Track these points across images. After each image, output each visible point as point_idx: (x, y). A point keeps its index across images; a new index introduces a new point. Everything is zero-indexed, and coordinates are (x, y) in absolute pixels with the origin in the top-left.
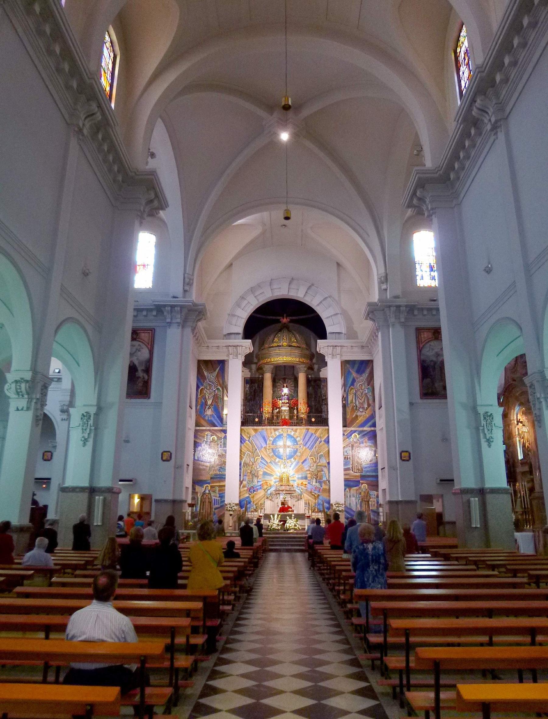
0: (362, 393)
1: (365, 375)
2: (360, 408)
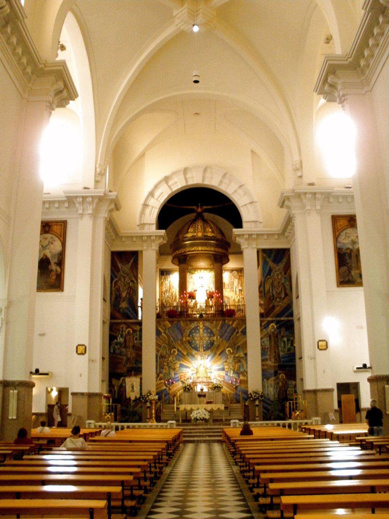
0: (279, 283)
1: (281, 265)
2: (276, 298)
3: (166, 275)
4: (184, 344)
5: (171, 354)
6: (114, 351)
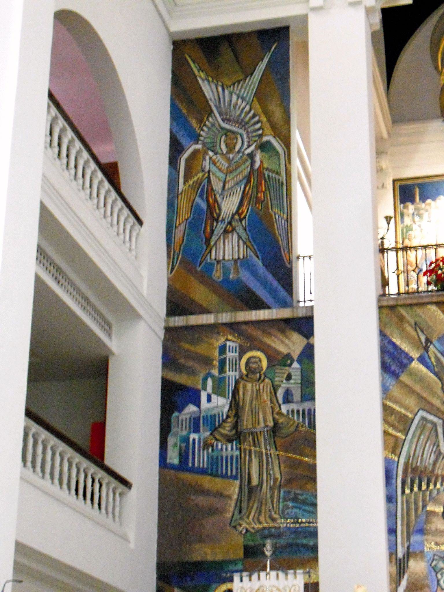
3: (423, 199)
6: (184, 456)
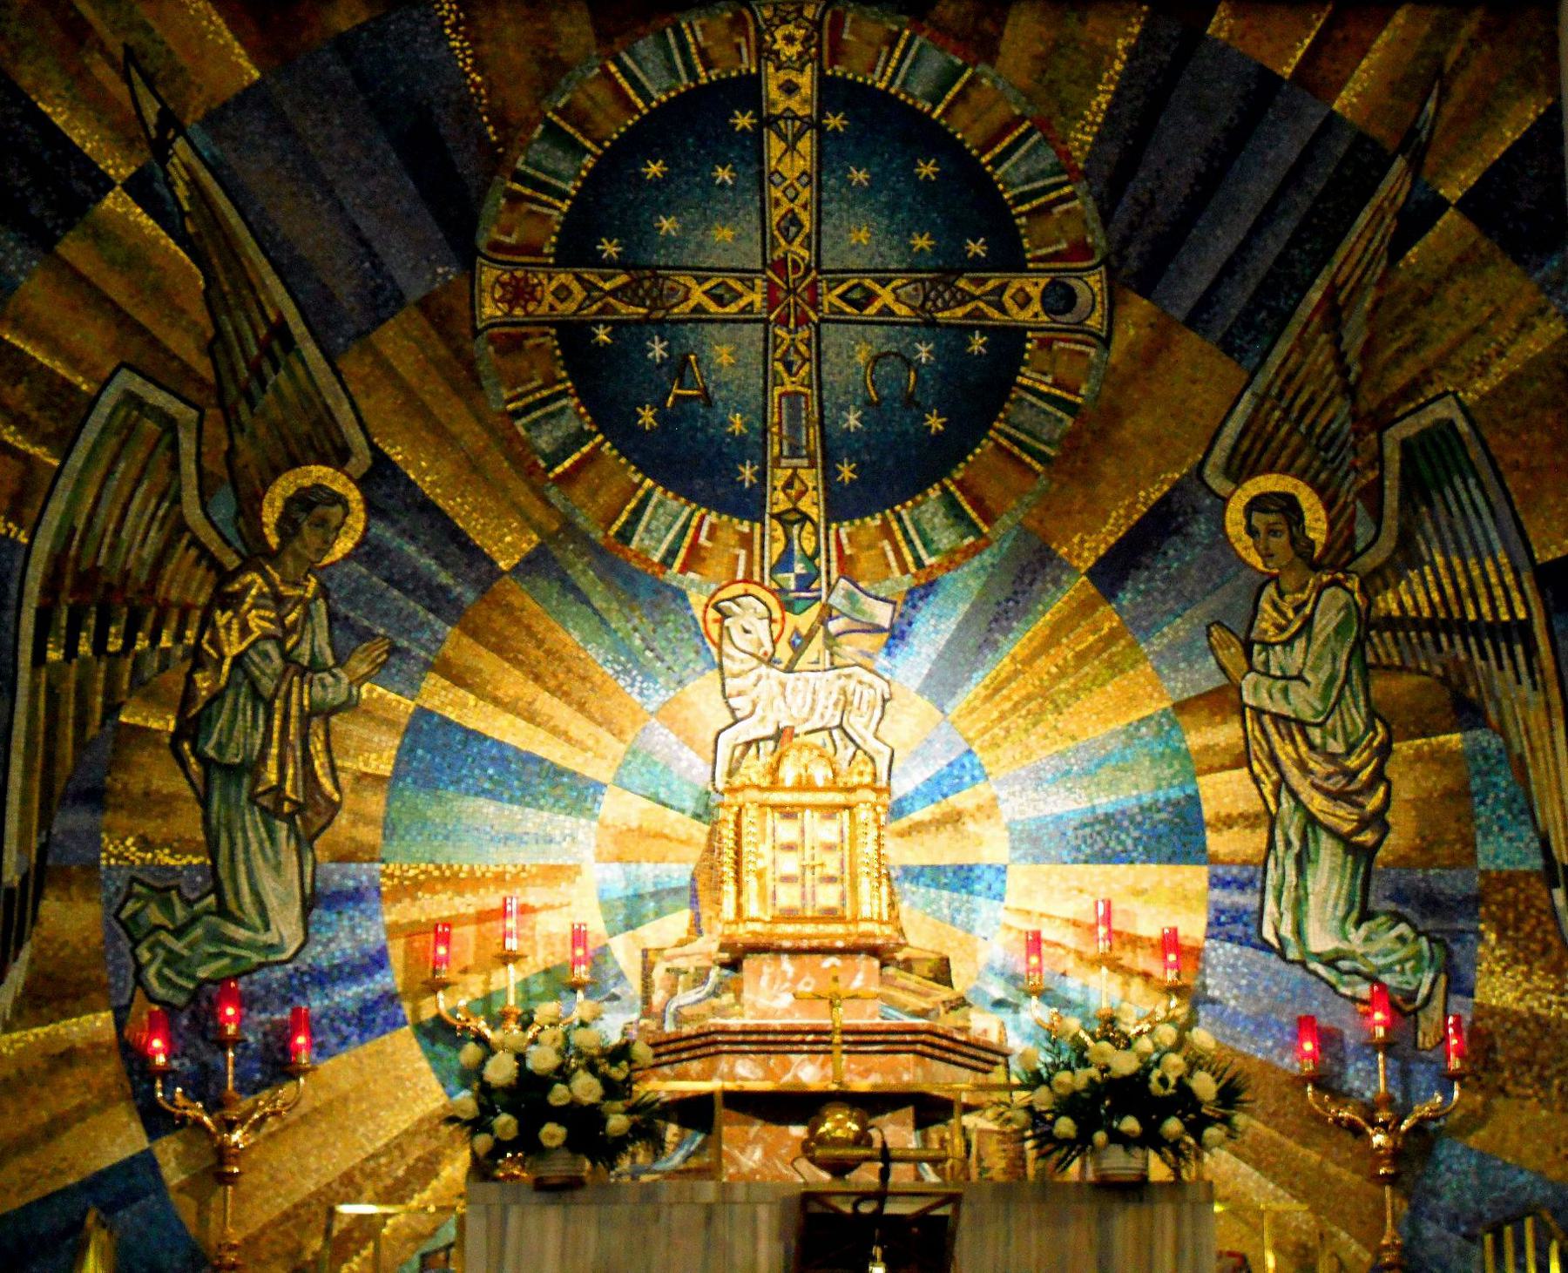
4: (502, 397)
5: (256, 555)
